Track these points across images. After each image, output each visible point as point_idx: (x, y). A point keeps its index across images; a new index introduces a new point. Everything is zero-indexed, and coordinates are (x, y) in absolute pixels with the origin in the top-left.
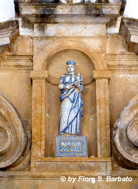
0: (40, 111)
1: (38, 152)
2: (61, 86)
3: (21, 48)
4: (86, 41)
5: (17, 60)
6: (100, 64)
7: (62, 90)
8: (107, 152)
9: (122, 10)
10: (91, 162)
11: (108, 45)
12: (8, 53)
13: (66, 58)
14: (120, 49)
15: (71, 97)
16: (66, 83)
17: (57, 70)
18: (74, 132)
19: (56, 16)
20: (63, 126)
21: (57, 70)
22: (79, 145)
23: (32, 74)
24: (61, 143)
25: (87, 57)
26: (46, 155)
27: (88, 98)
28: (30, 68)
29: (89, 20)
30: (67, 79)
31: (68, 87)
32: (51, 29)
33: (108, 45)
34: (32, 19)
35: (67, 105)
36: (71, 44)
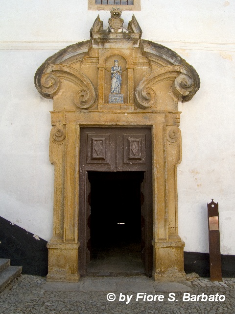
0: (102, 82)
1: (101, 101)
2: (112, 72)
3: (93, 54)
4: (124, 51)
5: (92, 60)
6: (130, 61)
7: (112, 74)
8: (132, 101)
9: (140, 36)
10: (124, 106)
11: (133, 53)
12: (87, 56)
13: (113, 59)
14: (139, 55)
15: (116, 76)
16: (114, 70)
17: (109, 64)
18: (117, 92)
19: (109, 39)
20: (112, 90)
21: (109, 64)
22: (119, 99)
23: (98, 66)
24: (111, 98)
25: (123, 58)
26: (105, 103)
27: (124, 77)
28: (98, 63)
29: (125, 40)
30: (115, 68)
31: (115, 72)
32: (107, 45)
33: (133, 53)
34: (98, 40)
35: (114, 80)
36: (116, 52)
